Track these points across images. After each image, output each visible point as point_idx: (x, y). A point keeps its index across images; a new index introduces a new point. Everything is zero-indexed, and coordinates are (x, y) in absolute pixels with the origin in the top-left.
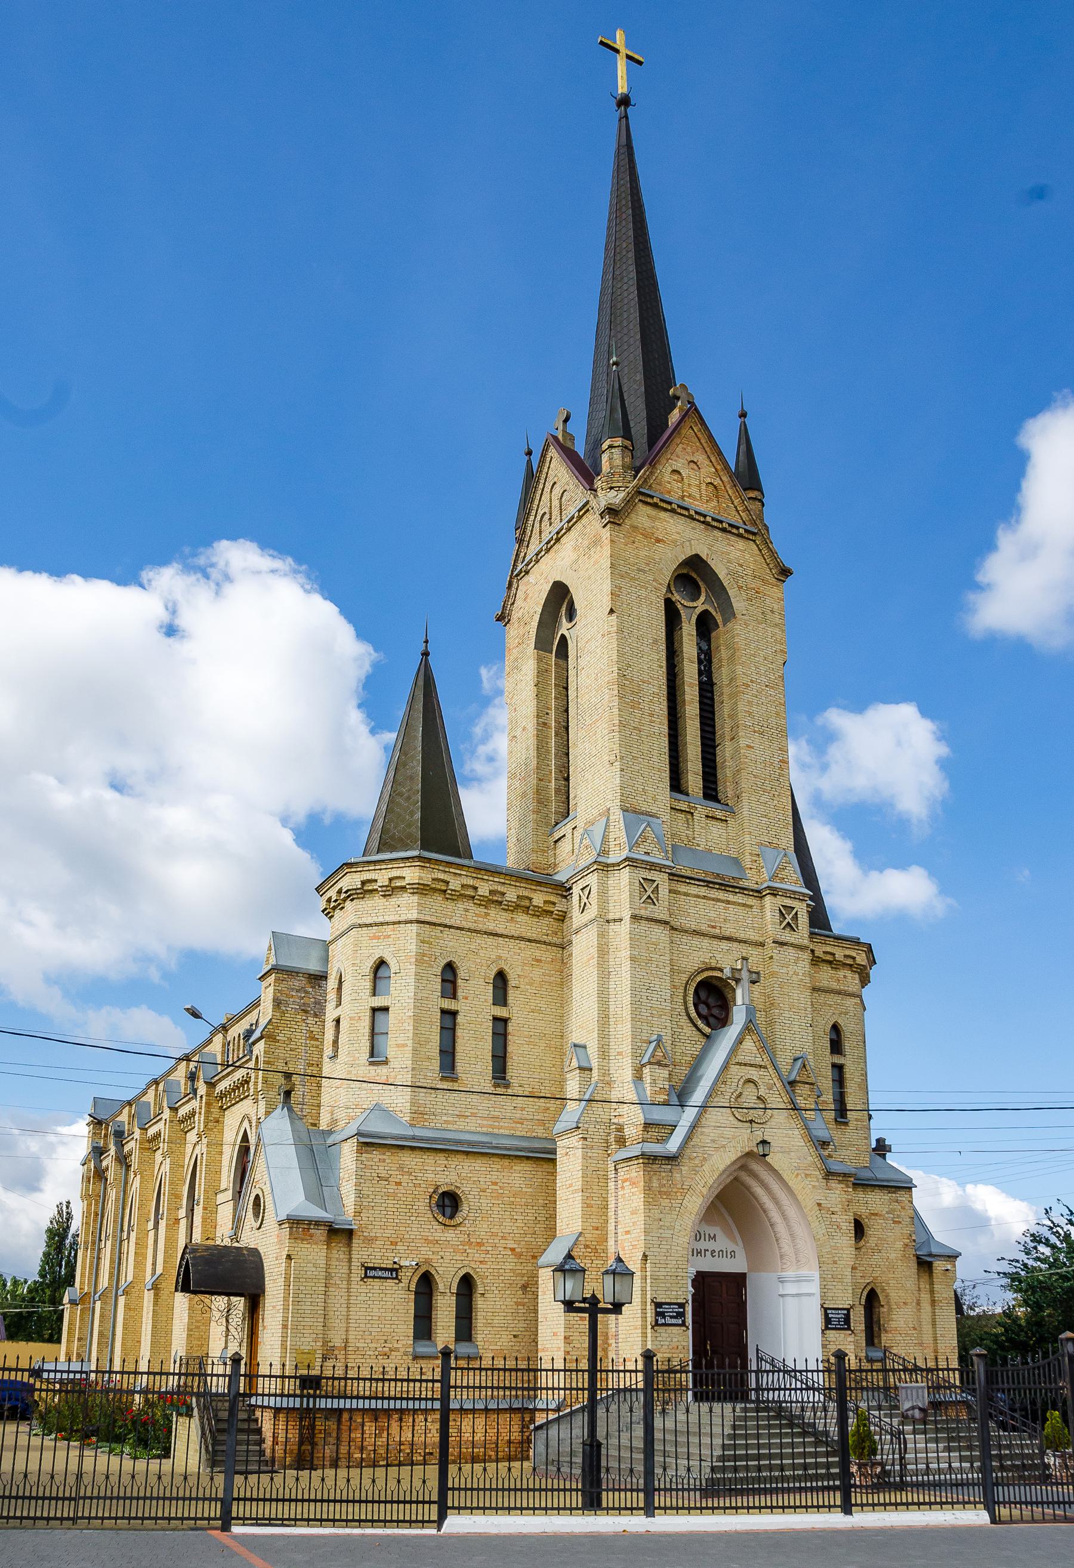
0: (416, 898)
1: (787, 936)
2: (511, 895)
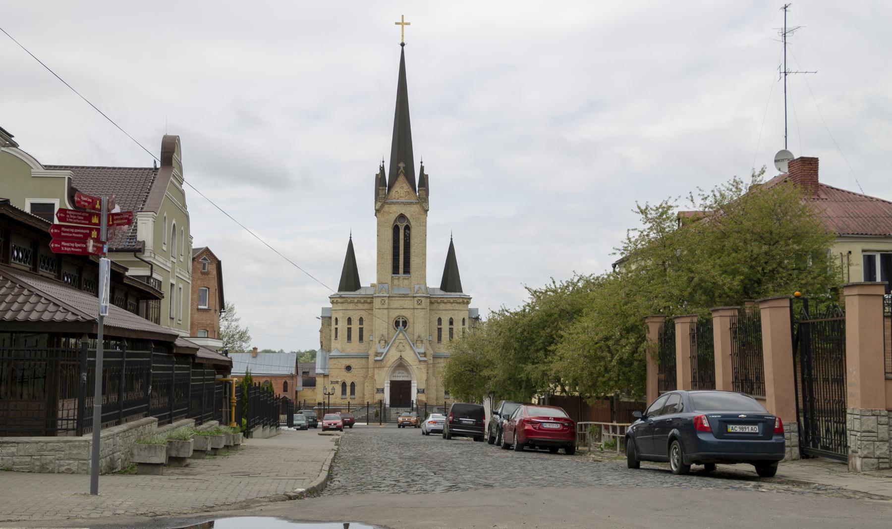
0: (342, 305)
1: (419, 307)
2: (362, 301)
